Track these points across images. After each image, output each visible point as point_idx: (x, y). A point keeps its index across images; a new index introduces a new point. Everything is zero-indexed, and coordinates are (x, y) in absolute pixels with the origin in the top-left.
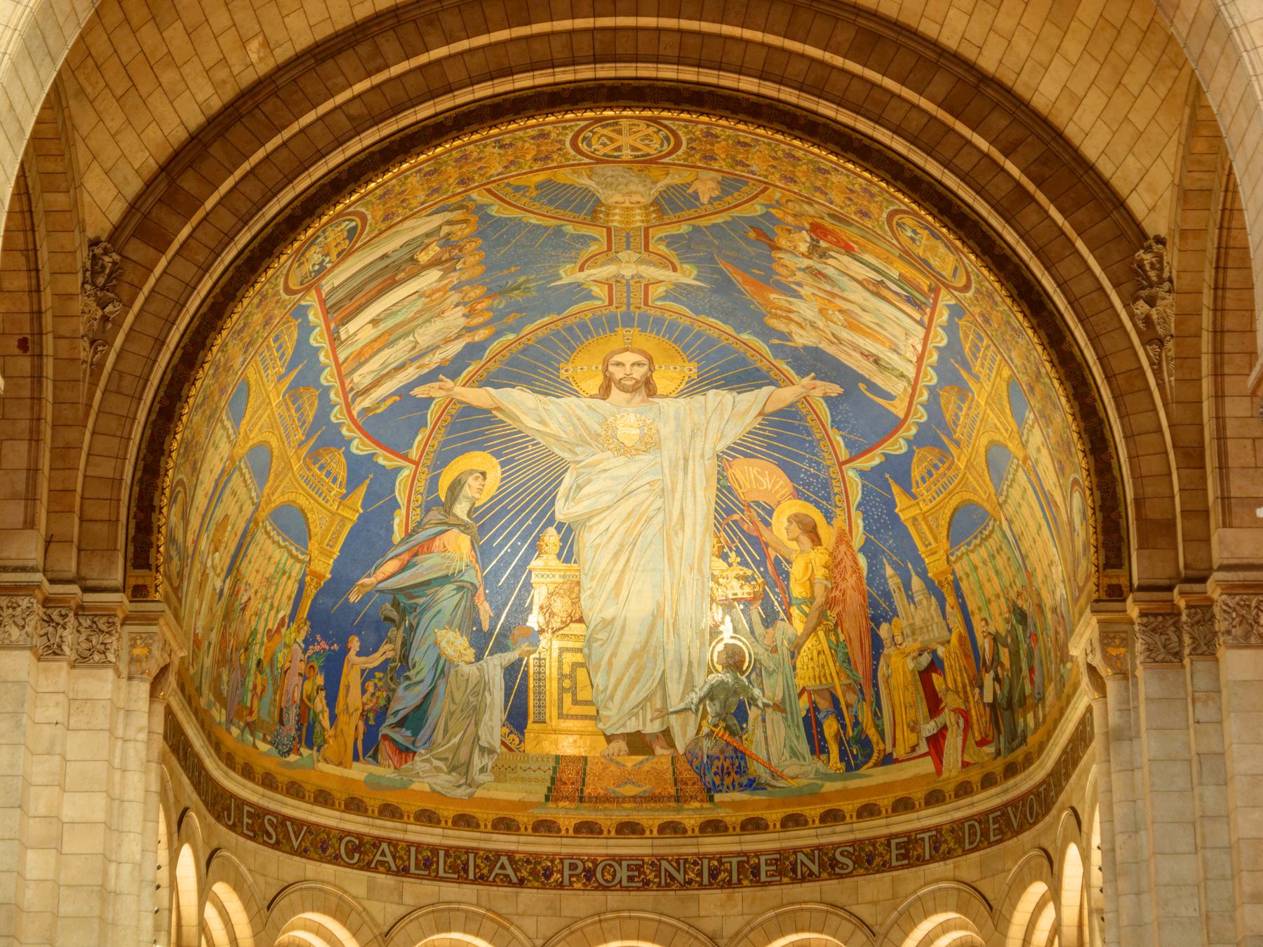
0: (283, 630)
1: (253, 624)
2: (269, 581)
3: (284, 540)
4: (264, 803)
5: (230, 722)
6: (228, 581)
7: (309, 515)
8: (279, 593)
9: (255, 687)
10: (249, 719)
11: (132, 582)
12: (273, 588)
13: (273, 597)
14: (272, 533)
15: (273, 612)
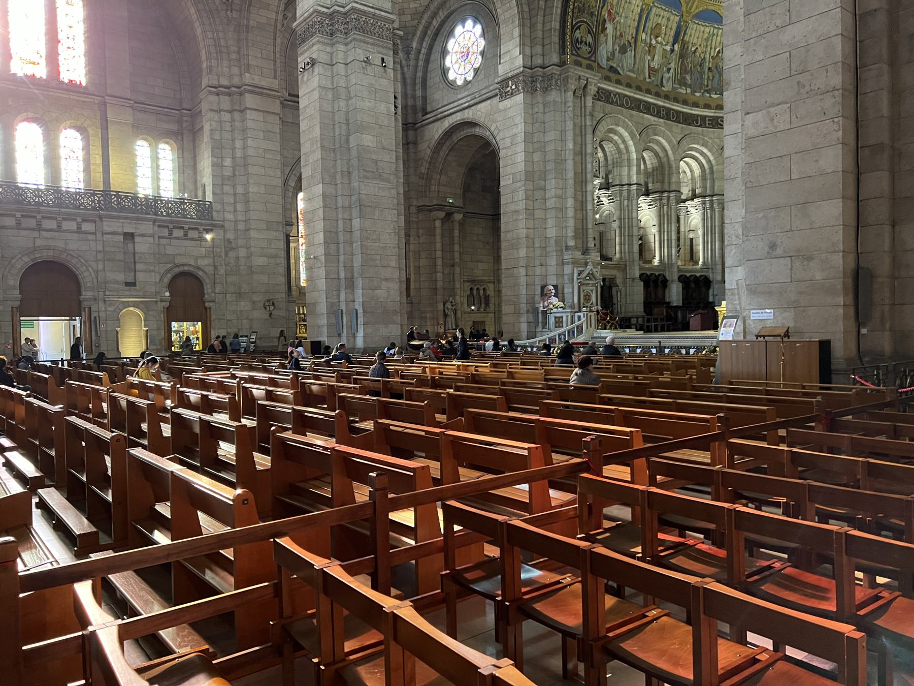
0: (720, 55)
1: (702, 56)
2: (707, 40)
3: (709, 24)
4: (716, 115)
5: (693, 92)
6: (676, 47)
7: (719, 12)
8: (714, 42)
9: (708, 77)
10: (706, 89)
11: (562, 60)
12: (710, 42)
13: (711, 45)
14: (700, 23)
15: (713, 50)
